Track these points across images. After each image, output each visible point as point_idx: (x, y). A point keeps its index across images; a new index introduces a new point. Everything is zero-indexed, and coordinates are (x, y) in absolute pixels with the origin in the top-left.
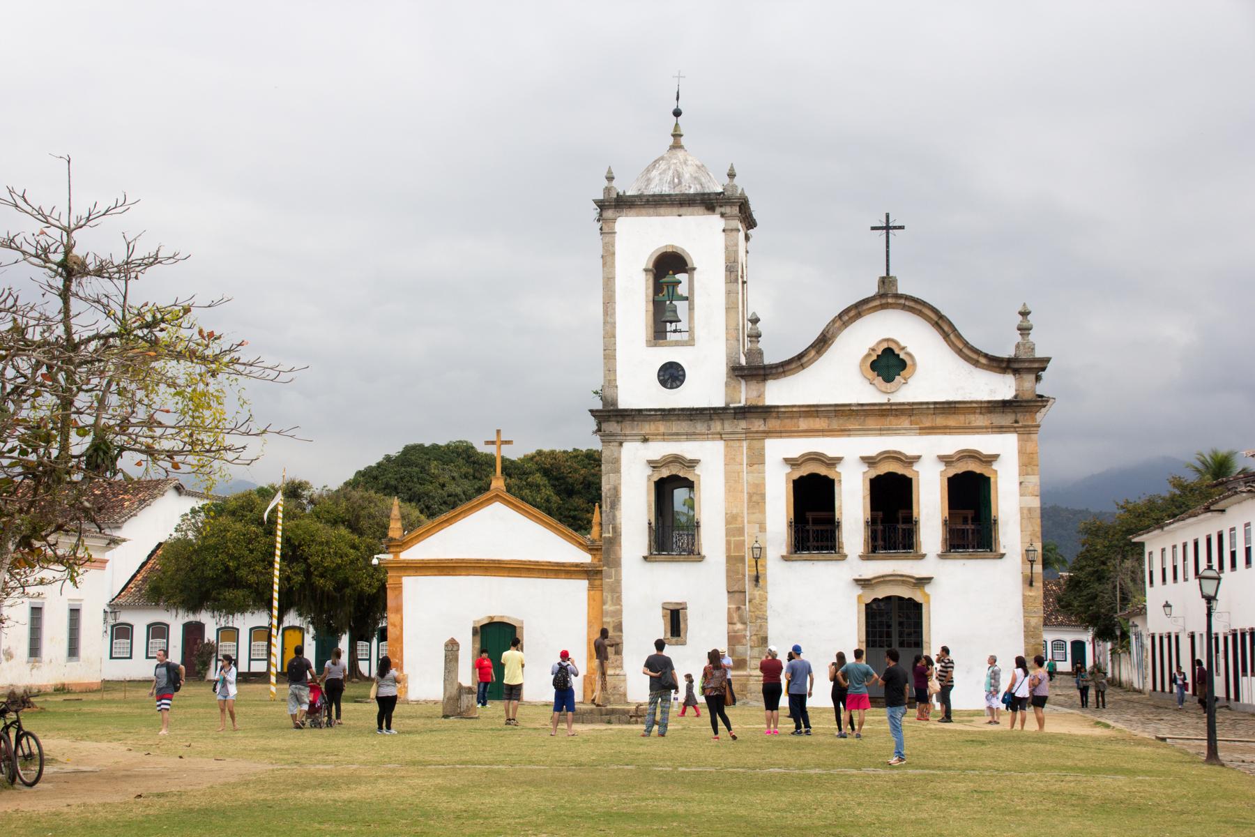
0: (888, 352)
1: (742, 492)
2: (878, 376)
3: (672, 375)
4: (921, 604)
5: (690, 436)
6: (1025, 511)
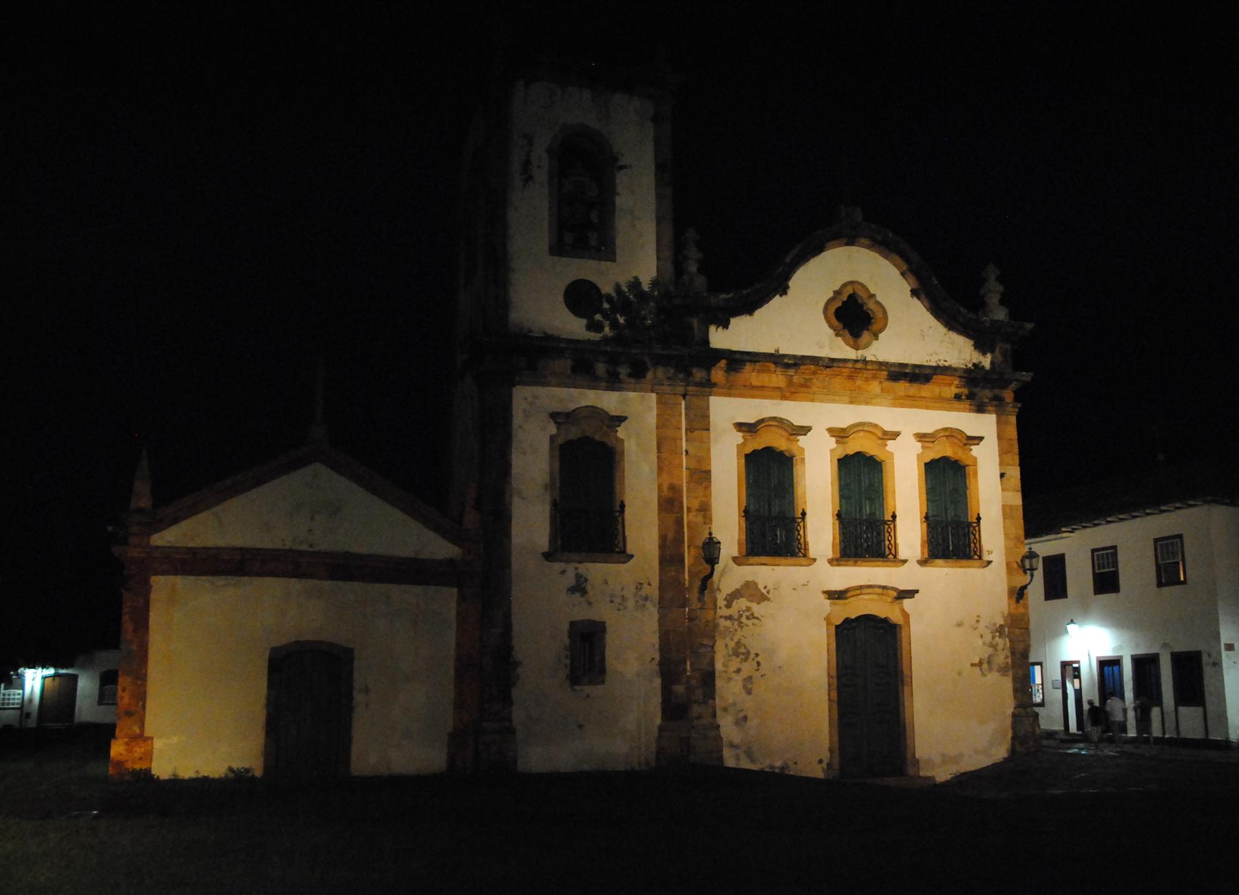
0: (852, 297)
1: (680, 465)
2: (844, 328)
4: (900, 626)
5: (613, 383)
6: (1008, 511)
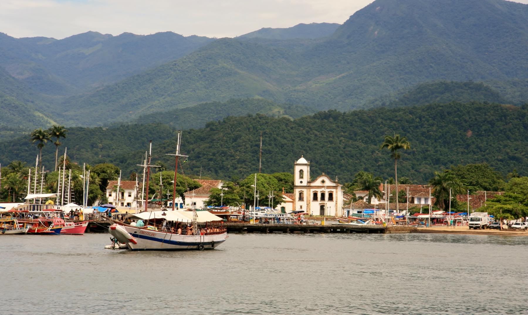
3: (301, 182)
5: (303, 188)
